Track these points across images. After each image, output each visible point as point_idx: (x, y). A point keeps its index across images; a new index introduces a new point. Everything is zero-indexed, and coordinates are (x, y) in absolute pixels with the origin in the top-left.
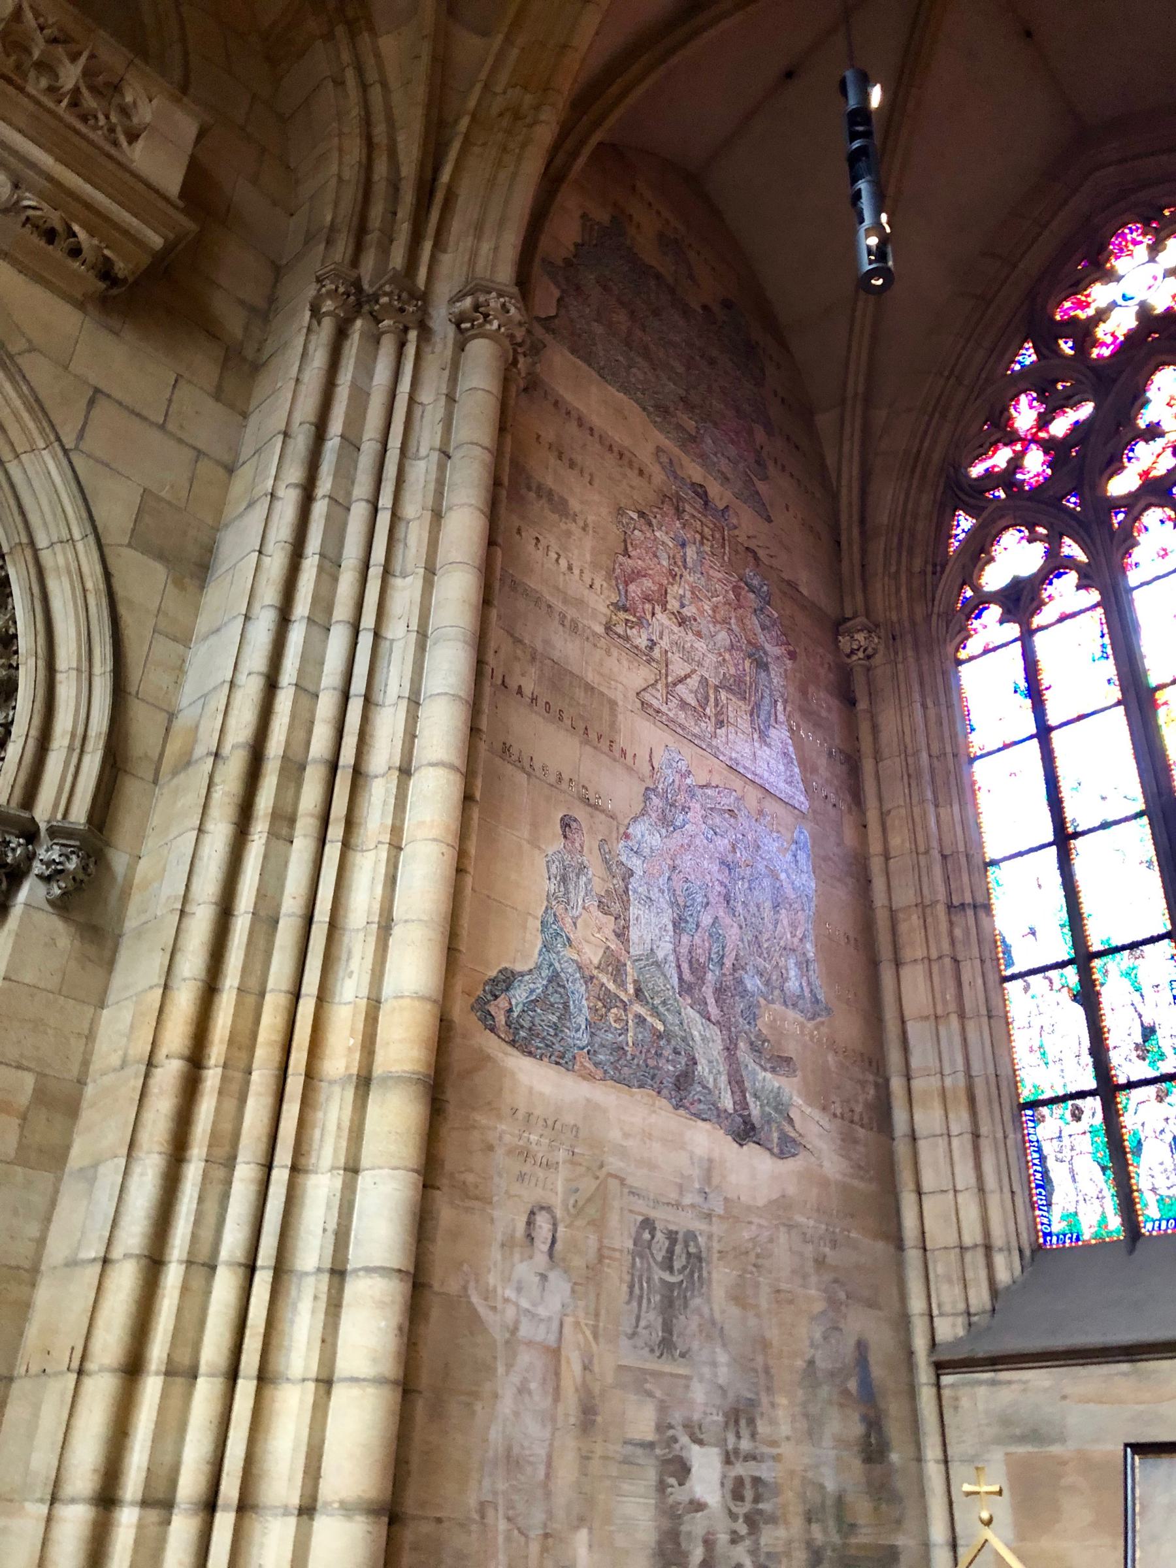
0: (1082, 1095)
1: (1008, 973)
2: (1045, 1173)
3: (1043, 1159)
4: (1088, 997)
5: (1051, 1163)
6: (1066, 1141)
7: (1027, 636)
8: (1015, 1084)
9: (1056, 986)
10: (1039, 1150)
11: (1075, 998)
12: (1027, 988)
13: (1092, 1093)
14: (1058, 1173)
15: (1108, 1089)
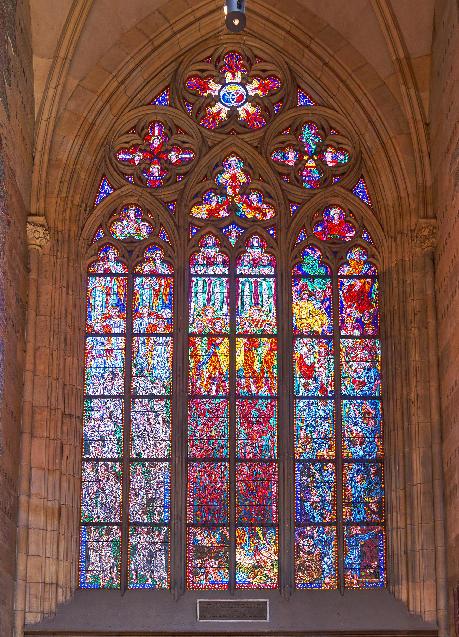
0: (113, 524)
1: (86, 457)
2: (87, 556)
3: (87, 550)
4: (124, 479)
5: (91, 552)
6: (101, 544)
7: (131, 275)
8: (80, 512)
9: (110, 469)
10: (86, 546)
11: (117, 478)
12: (94, 467)
13: (117, 524)
14: (93, 557)
15: (126, 525)
